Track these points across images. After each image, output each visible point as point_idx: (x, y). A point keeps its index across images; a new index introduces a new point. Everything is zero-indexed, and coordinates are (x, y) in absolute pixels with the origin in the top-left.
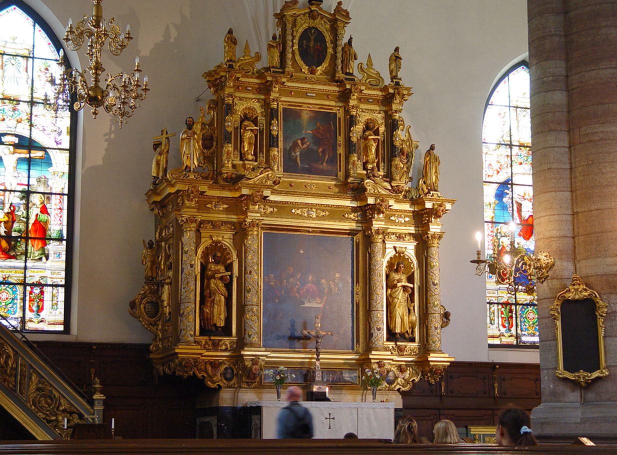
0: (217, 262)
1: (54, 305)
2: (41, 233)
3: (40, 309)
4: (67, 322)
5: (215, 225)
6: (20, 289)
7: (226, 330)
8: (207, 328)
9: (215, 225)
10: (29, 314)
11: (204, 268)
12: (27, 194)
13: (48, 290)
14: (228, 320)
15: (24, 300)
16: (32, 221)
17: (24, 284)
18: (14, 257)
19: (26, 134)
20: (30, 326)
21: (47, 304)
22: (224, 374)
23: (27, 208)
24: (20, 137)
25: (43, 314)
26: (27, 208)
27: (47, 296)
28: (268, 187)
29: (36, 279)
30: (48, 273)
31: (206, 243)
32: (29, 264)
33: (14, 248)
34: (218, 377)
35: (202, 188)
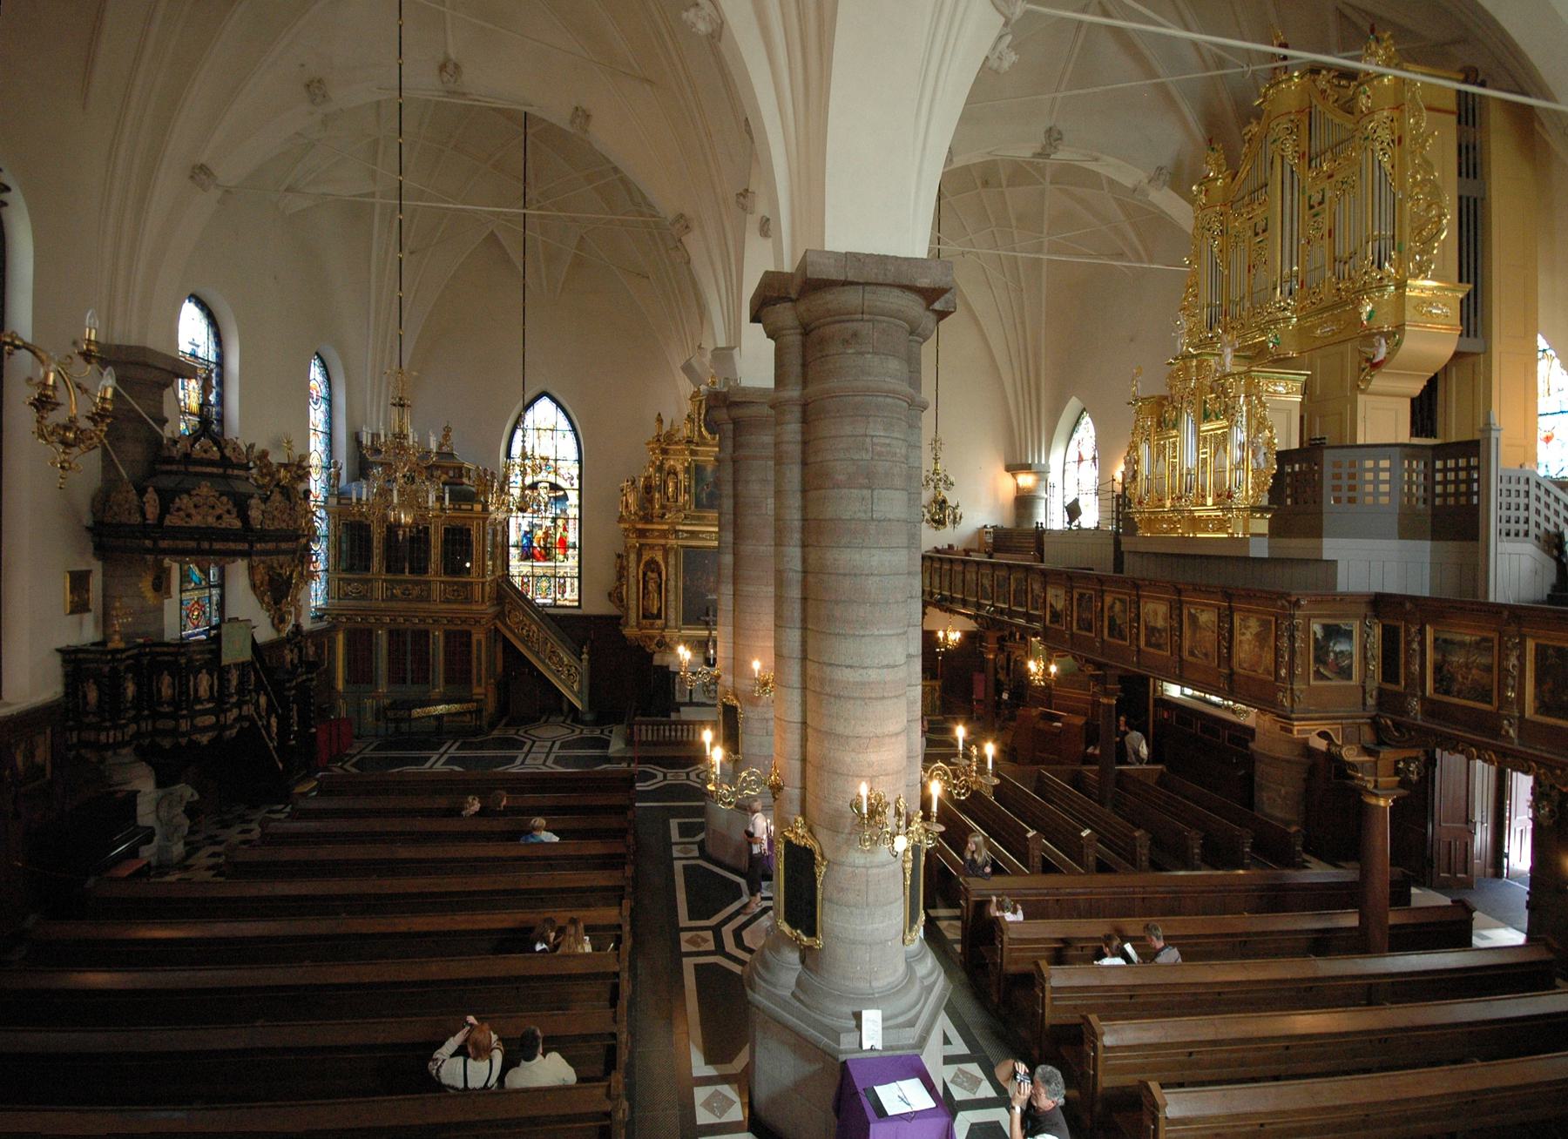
0: (653, 571)
1: (572, 591)
2: (563, 544)
3: (564, 592)
4: (579, 600)
5: (652, 547)
6: (552, 580)
7: (659, 616)
8: (647, 615)
9: (652, 547)
10: (558, 596)
11: (645, 574)
12: (554, 520)
13: (568, 580)
14: (660, 609)
15: (555, 587)
16: (558, 536)
17: (555, 577)
18: (550, 560)
19: (553, 481)
20: (559, 603)
21: (568, 589)
22: (657, 644)
23: (555, 528)
24: (551, 484)
25: (566, 595)
26: (555, 528)
27: (568, 584)
28: (679, 524)
29: (561, 574)
30: (568, 570)
31: (646, 557)
32: (558, 564)
33: (548, 554)
34: (653, 646)
35: (640, 526)
